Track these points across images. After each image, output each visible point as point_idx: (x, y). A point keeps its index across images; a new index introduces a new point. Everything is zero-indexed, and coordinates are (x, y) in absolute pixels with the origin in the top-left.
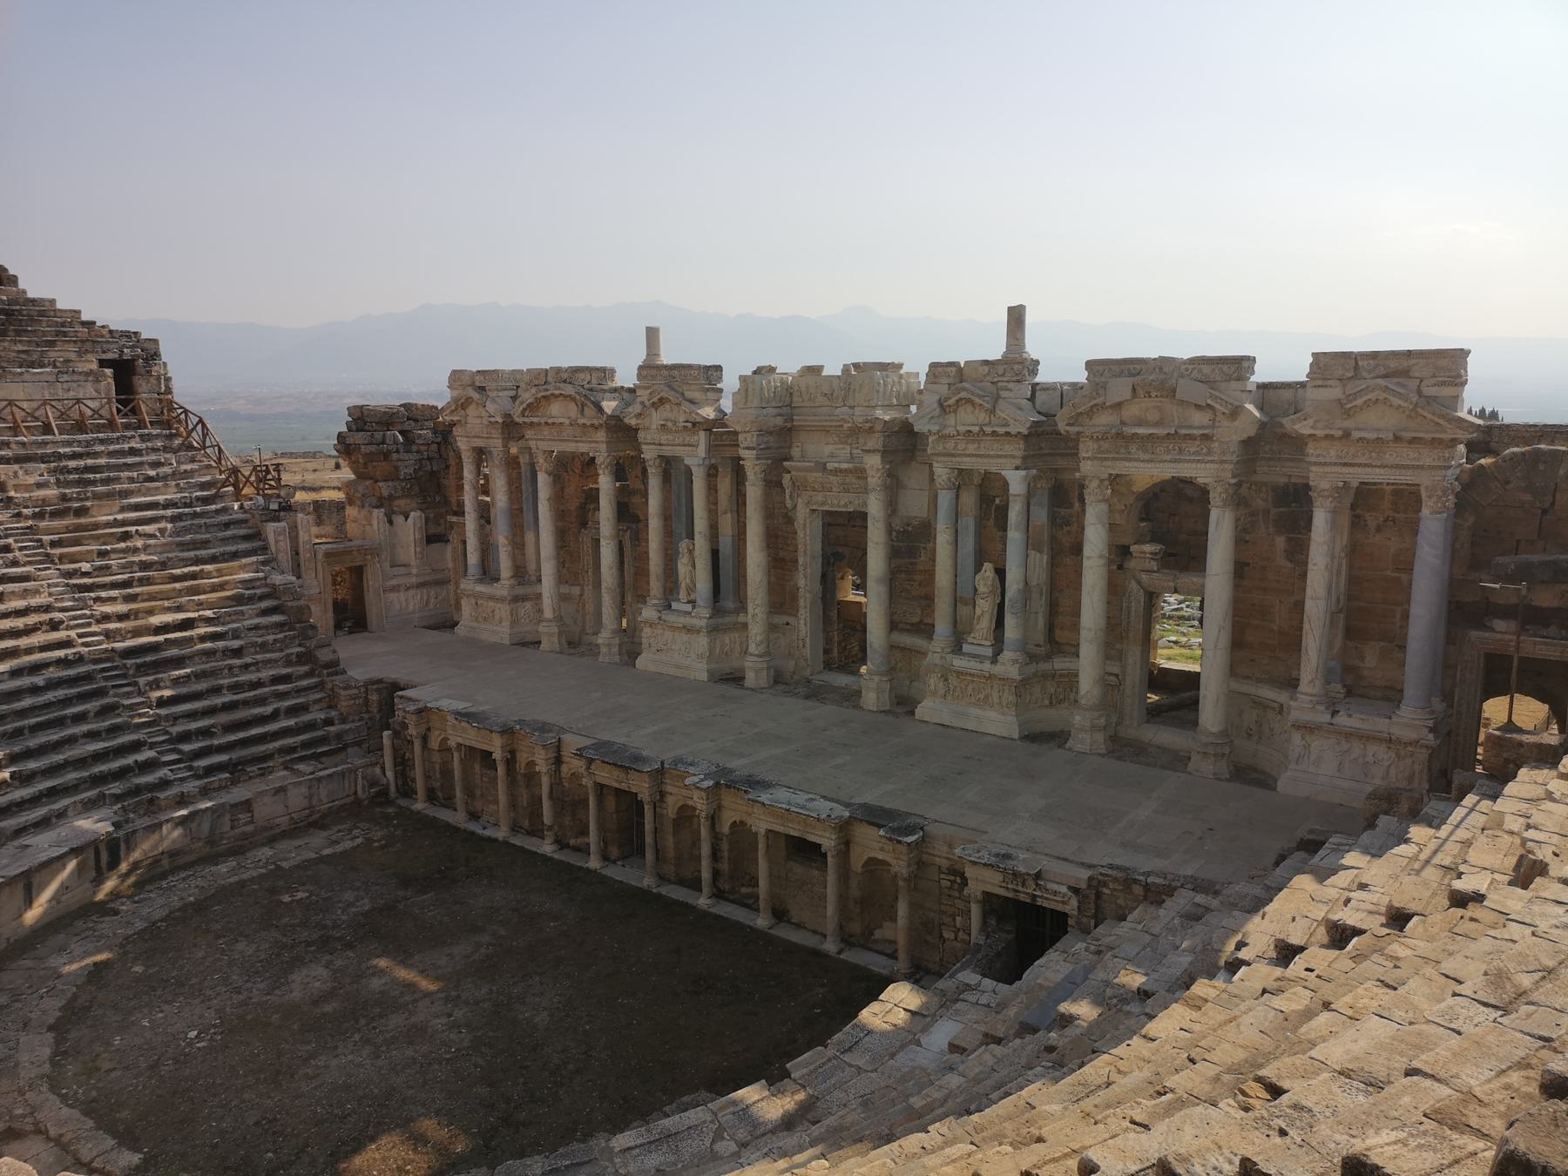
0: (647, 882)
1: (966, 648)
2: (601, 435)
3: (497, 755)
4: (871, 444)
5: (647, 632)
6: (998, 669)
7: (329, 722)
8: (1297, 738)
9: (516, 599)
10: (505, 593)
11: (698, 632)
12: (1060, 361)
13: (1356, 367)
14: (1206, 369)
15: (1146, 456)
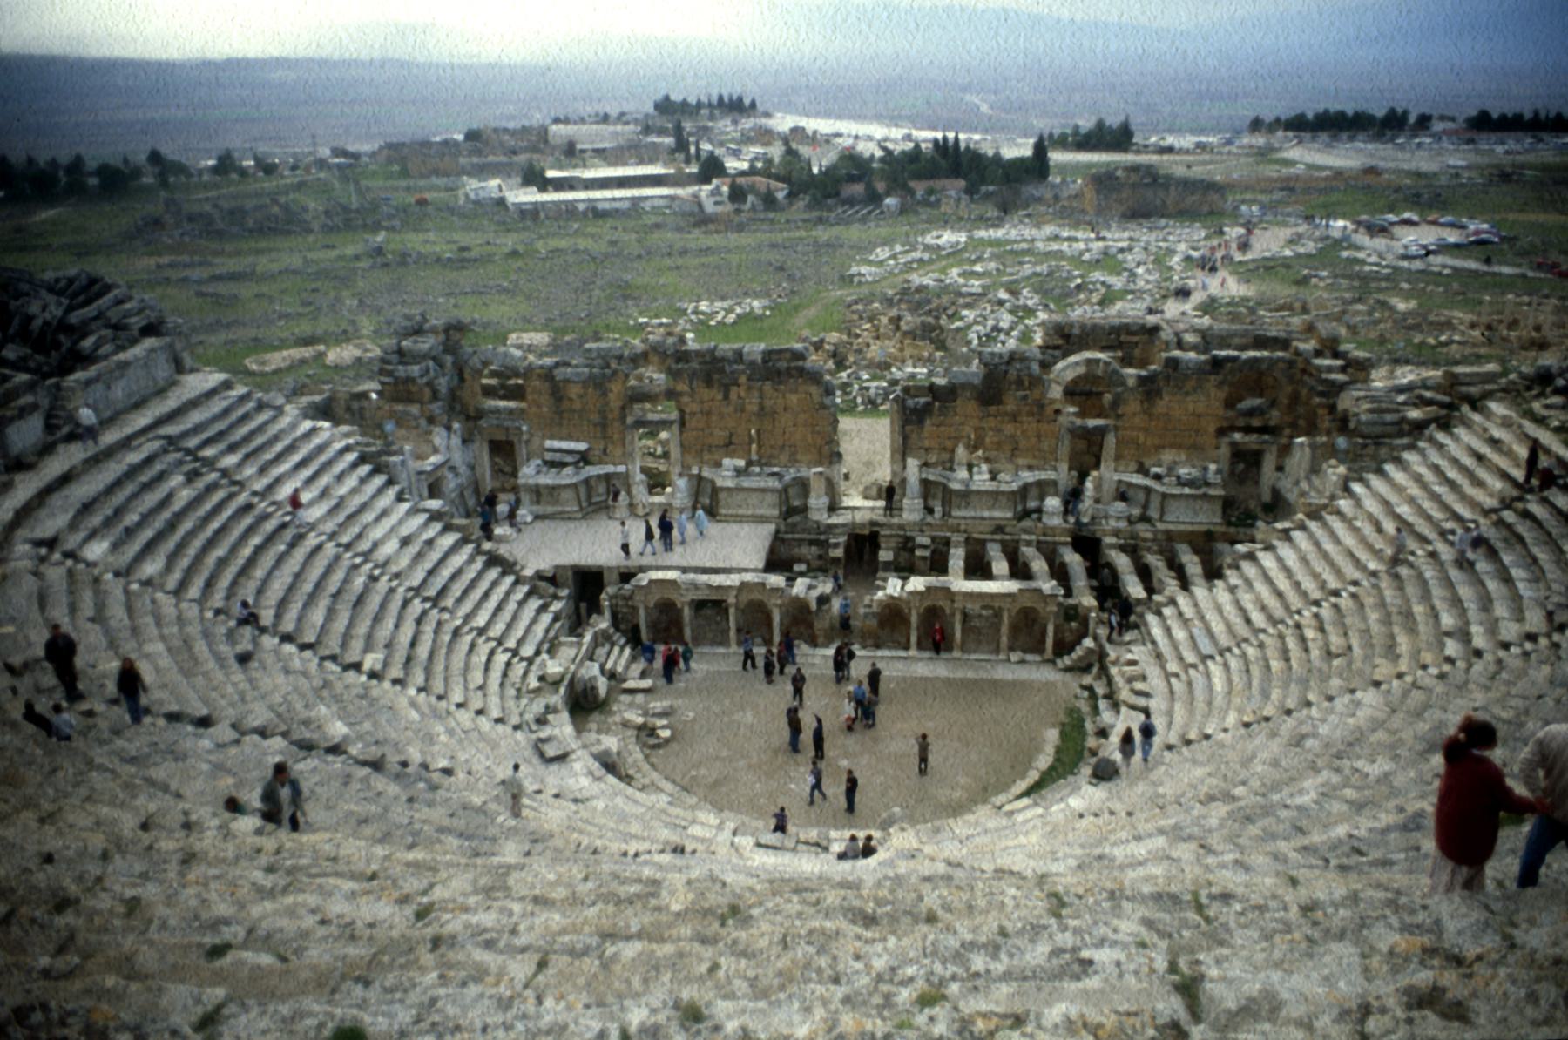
3: (731, 600)
6: (1004, 488)
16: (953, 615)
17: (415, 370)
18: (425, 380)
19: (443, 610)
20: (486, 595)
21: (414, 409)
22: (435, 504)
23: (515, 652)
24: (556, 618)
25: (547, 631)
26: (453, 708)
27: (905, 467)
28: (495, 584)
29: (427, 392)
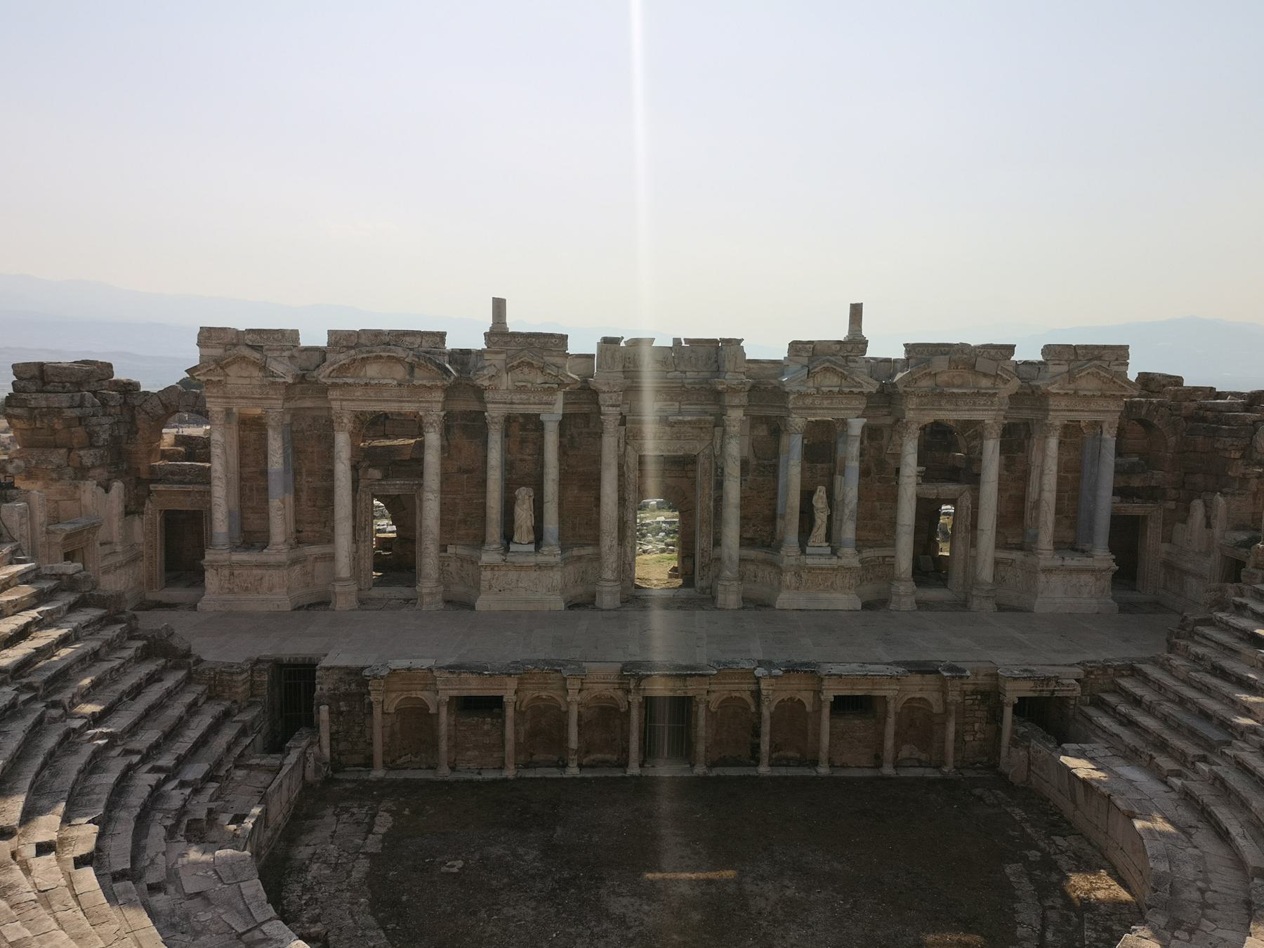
0: (700, 770)
1: (808, 550)
2: (438, 396)
3: (509, 697)
4: (736, 401)
5: (487, 575)
6: (843, 562)
7: (227, 715)
8: (1042, 577)
9: (294, 562)
10: (283, 558)
11: (552, 567)
12: (885, 343)
13: (1076, 353)
14: (993, 352)
15: (952, 407)
16: (818, 711)
17: (61, 400)
18: (77, 412)
19: (55, 705)
20: (136, 691)
21: (58, 457)
22: (71, 568)
23: (171, 773)
24: (243, 732)
25: (229, 749)
26: (29, 851)
27: (717, 542)
28: (152, 679)
29: (79, 432)
